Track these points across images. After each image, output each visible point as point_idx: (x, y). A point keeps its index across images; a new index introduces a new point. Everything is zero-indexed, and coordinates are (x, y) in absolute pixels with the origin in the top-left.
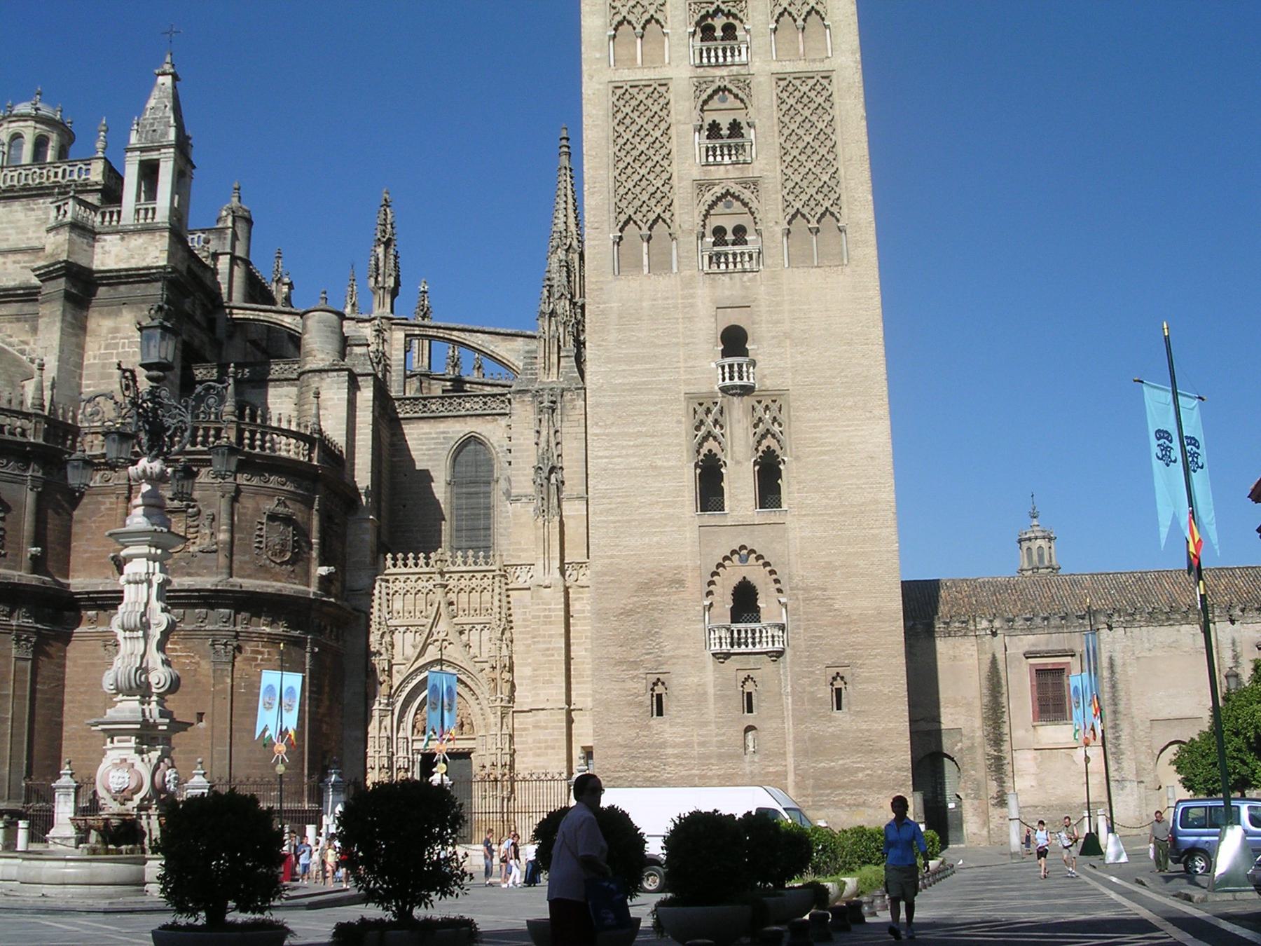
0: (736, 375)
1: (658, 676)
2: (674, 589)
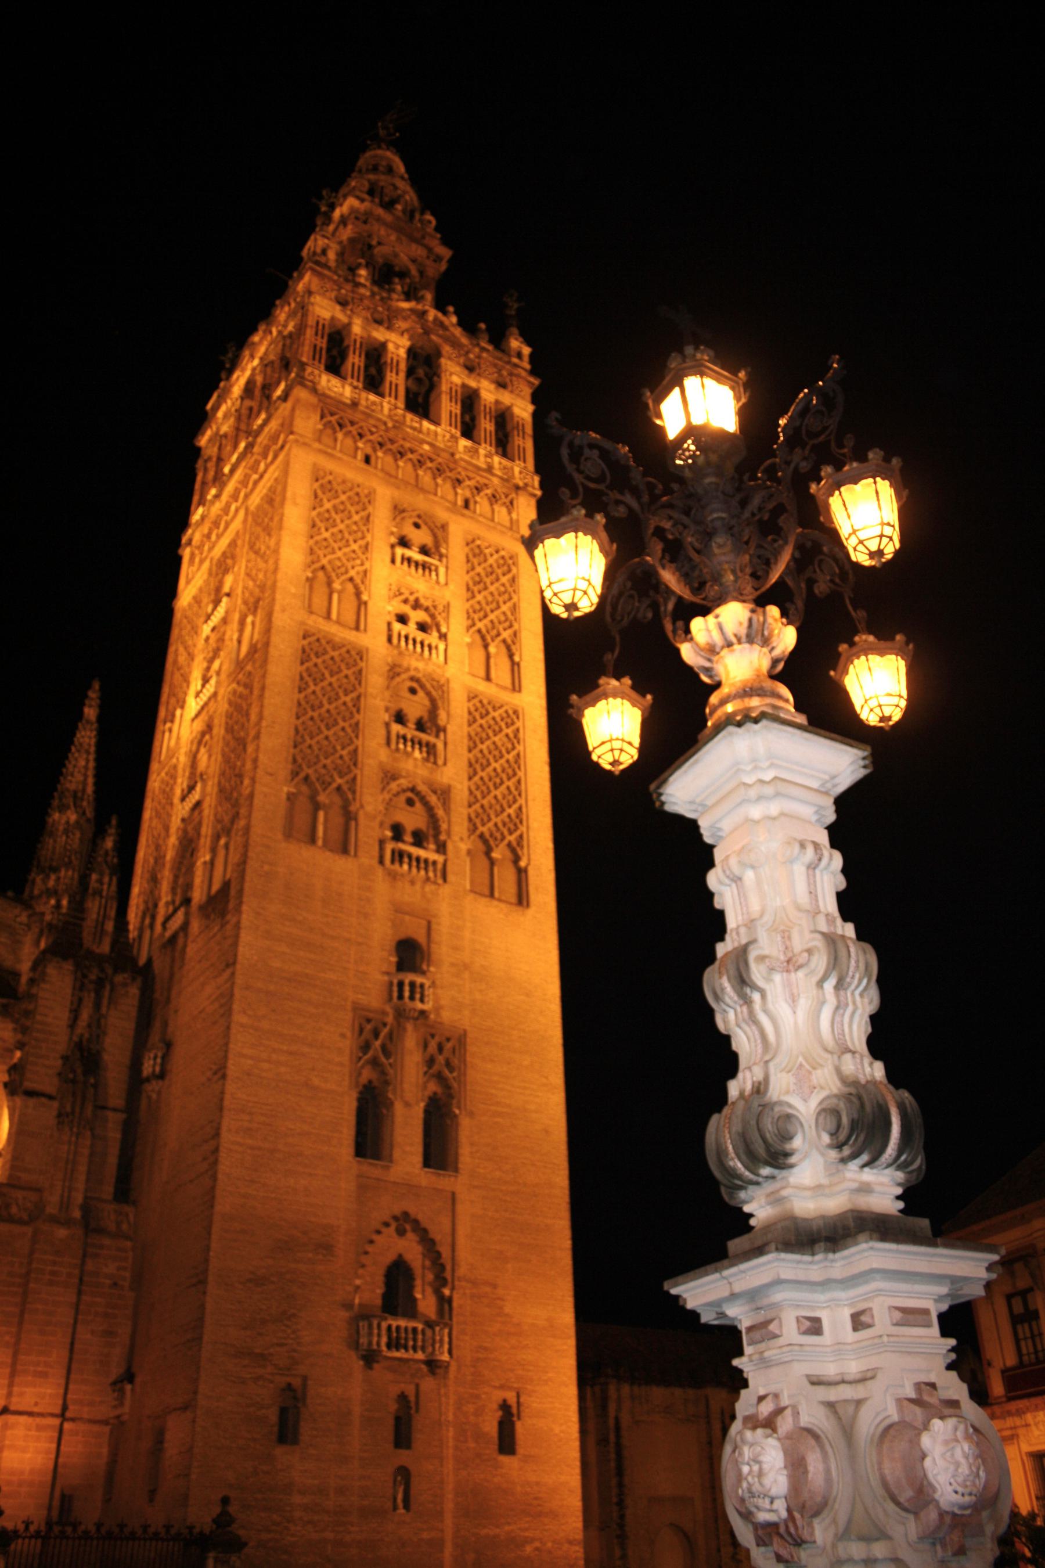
0: (418, 996)
1: (289, 1379)
2: (321, 1257)
